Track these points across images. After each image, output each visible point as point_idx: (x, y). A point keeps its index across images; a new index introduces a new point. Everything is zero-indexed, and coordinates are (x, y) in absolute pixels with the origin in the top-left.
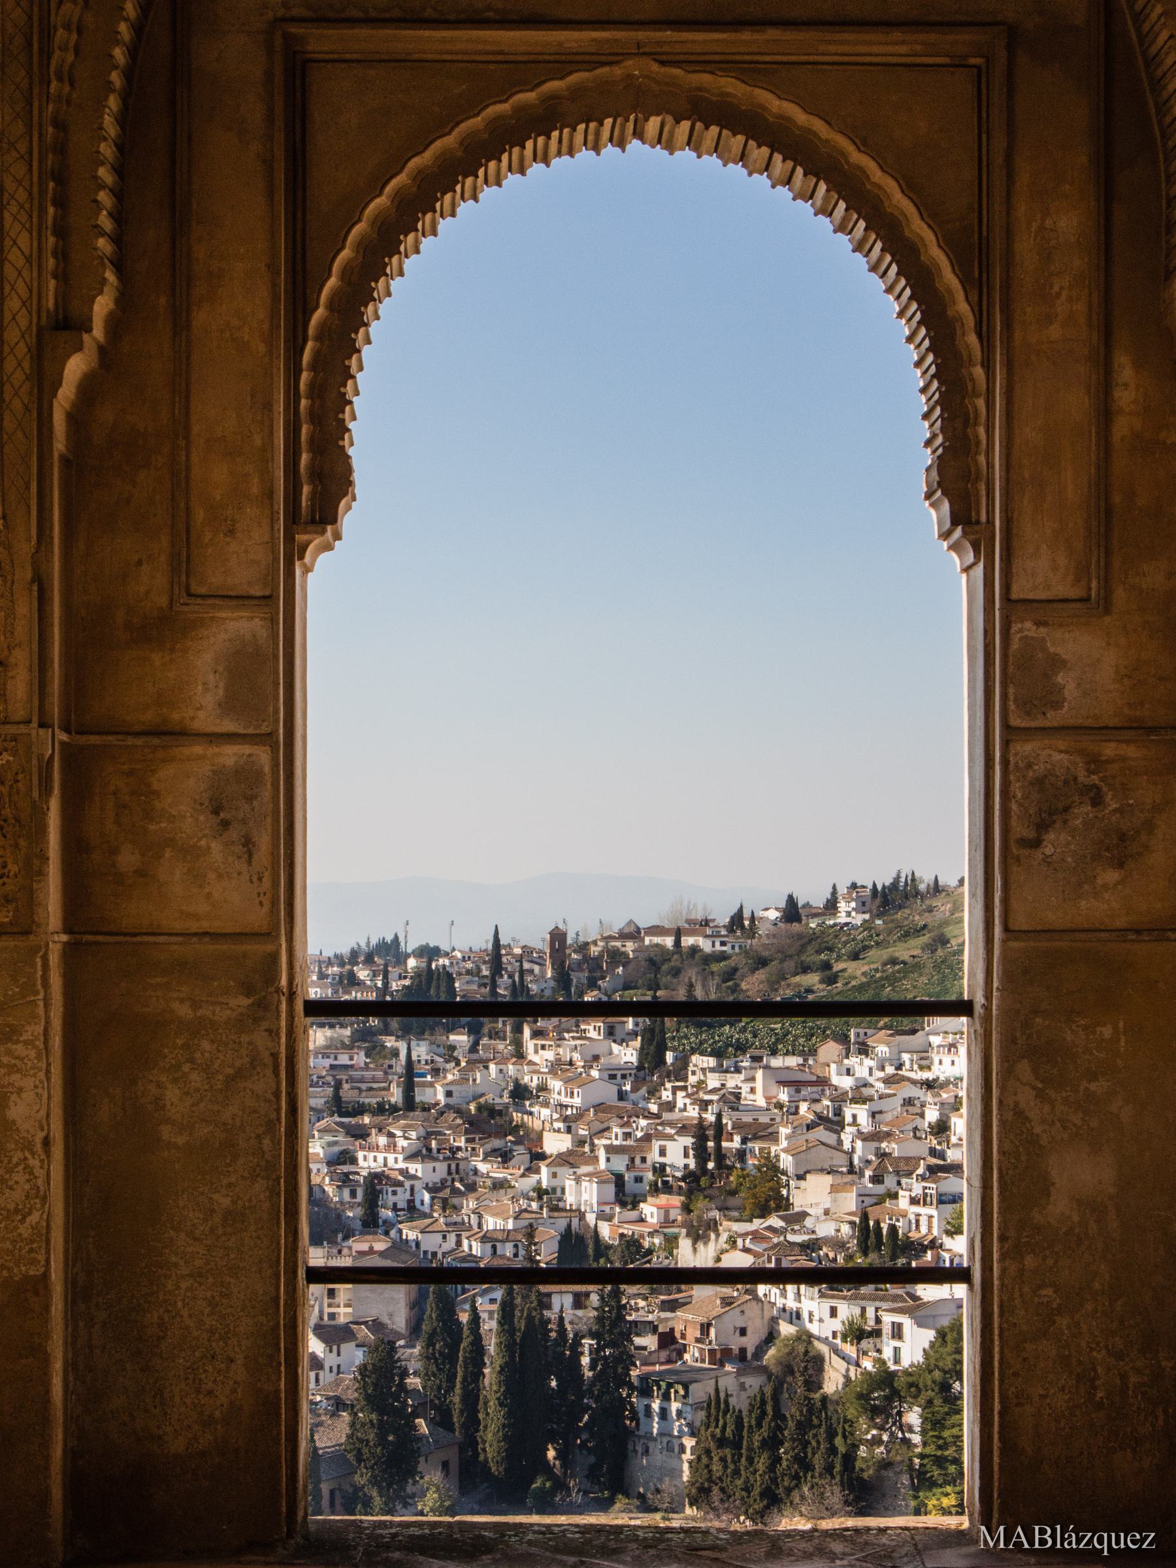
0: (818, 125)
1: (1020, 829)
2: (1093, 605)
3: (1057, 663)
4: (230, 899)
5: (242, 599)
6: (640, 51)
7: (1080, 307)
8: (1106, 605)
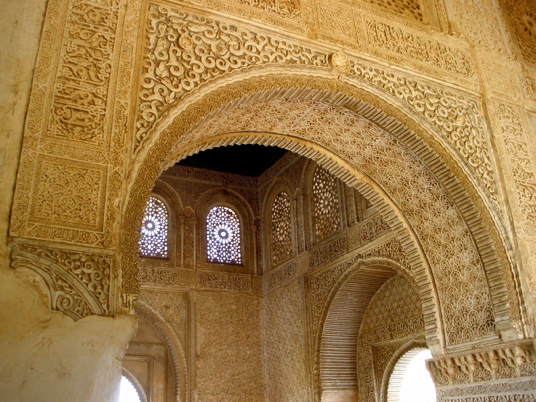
7: (163, 398)
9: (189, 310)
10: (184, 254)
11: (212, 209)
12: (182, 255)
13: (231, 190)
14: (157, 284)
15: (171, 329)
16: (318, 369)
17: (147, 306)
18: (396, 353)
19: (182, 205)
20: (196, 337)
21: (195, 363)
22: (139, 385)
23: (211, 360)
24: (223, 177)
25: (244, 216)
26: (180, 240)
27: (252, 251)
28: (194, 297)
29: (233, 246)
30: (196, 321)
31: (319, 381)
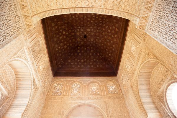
9: (106, 105)
16: (143, 107)
18: (164, 93)
20: (109, 111)
25: (116, 84)
27: (120, 90)
28: (107, 102)
31: (145, 110)
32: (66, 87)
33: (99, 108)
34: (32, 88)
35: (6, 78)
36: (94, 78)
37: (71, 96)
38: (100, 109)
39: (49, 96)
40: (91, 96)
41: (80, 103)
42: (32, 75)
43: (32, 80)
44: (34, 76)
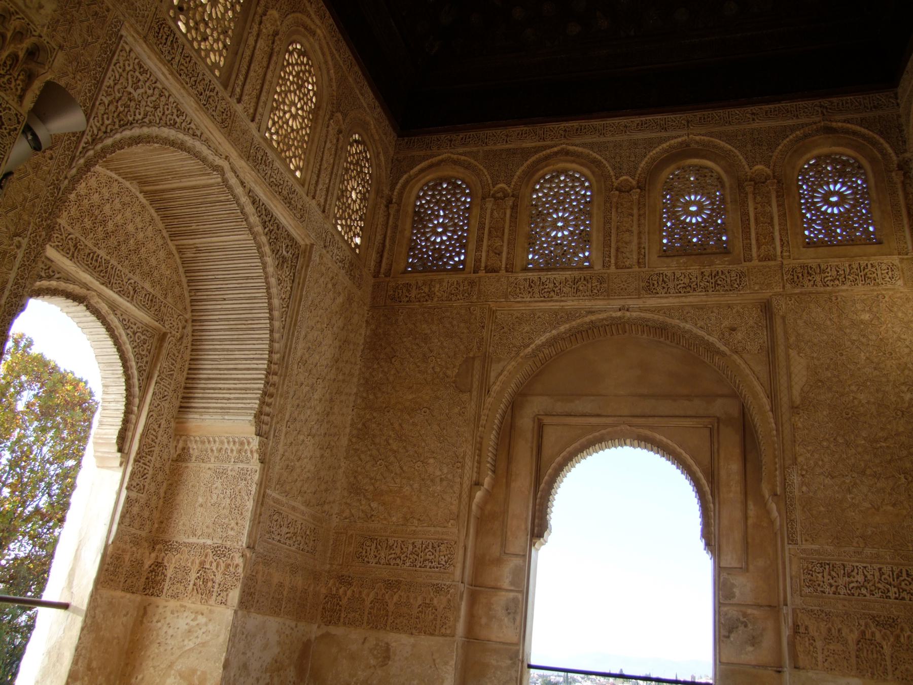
0: (669, 442)
1: (724, 632)
2: (745, 569)
3: (733, 585)
4: (508, 634)
5: (517, 555)
6: (624, 423)
8: (747, 570)
10: (757, 240)
11: (807, 162)
12: (754, 242)
13: (840, 124)
14: (710, 292)
15: (743, 366)
17: (695, 330)
19: (746, 166)
21: (790, 420)
22: (695, 468)
23: (825, 413)
24: (821, 106)
25: (873, 161)
26: (748, 220)
29: (856, 216)
30: (788, 347)
32: (489, 205)
33: (719, 352)
34: (270, 270)
35: (113, 241)
36: (699, 114)
37: (526, 269)
38: (723, 354)
39: (388, 274)
40: (669, 267)
41: (593, 318)
42: (239, 190)
43: (254, 219)
44: (261, 193)
